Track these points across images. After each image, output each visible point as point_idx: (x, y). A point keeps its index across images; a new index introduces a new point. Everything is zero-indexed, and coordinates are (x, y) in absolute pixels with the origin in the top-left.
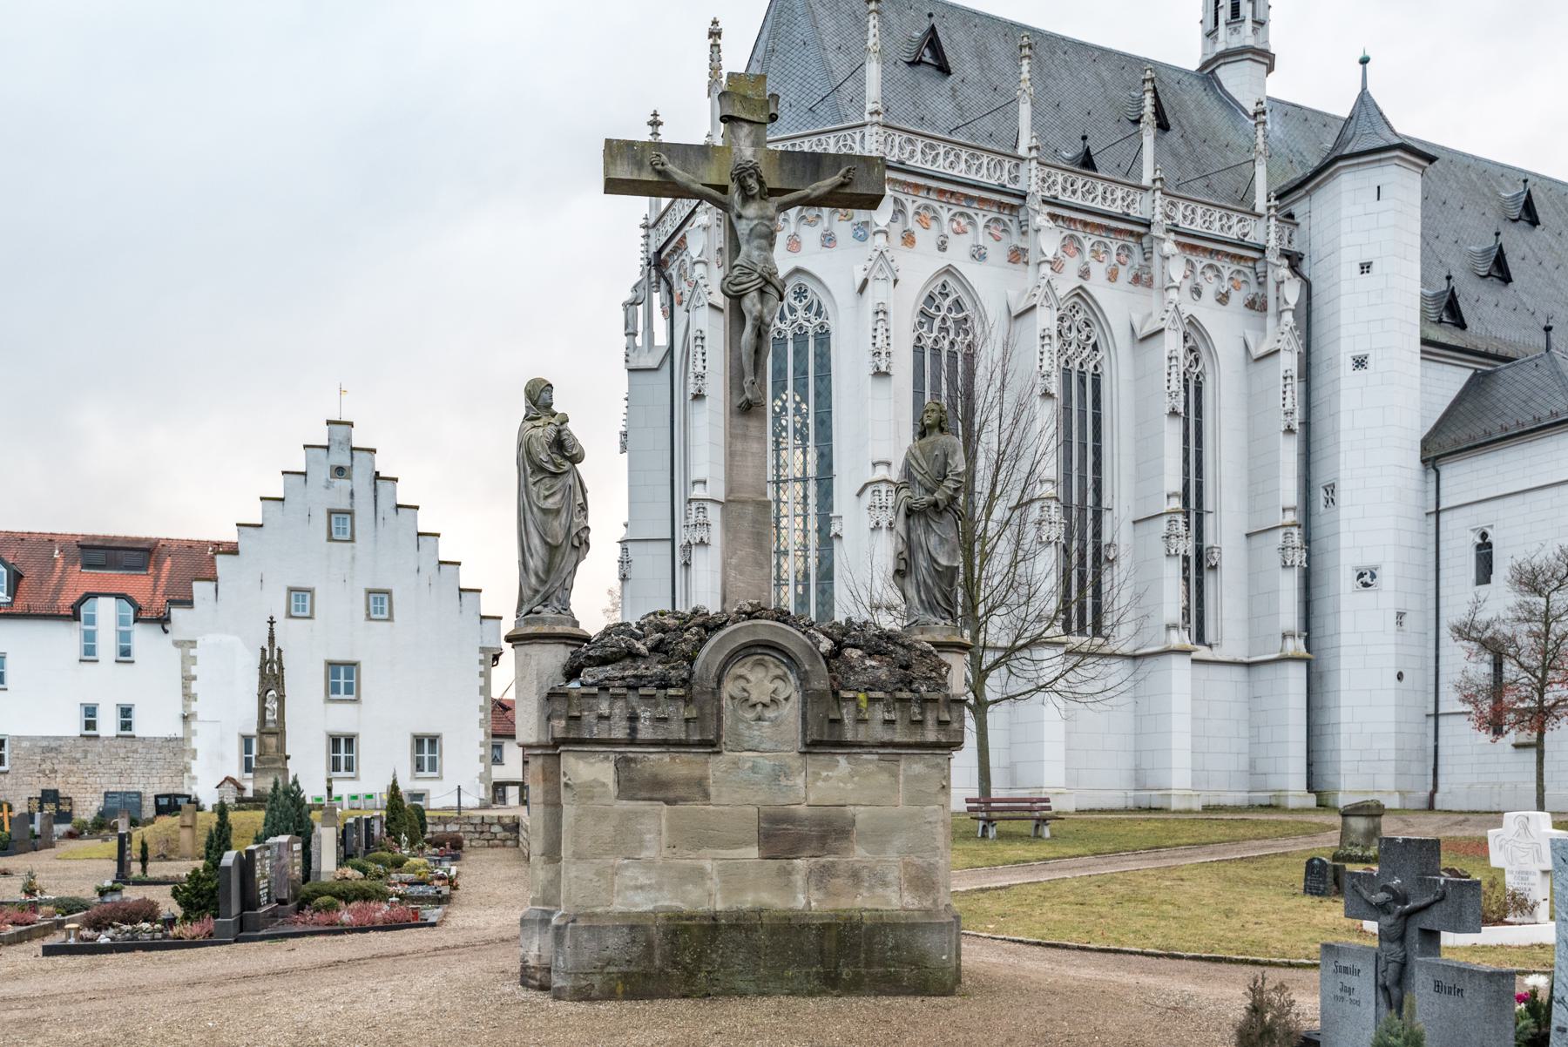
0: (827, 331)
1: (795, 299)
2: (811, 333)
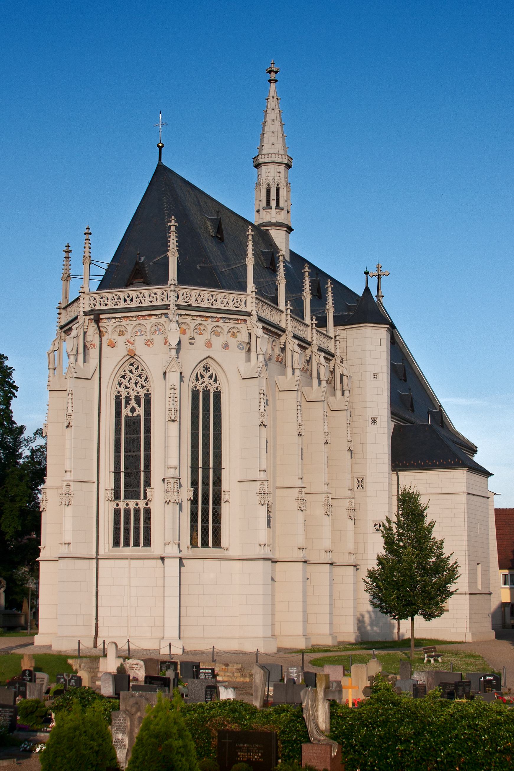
0: (220, 391)
1: (204, 371)
2: (212, 390)
